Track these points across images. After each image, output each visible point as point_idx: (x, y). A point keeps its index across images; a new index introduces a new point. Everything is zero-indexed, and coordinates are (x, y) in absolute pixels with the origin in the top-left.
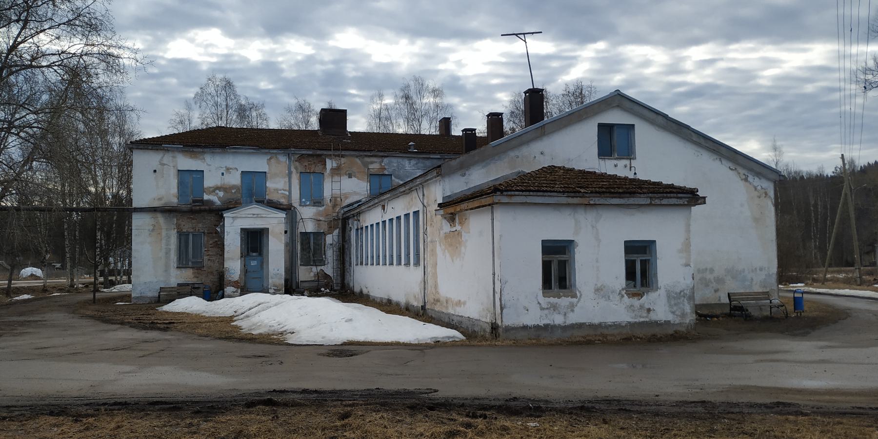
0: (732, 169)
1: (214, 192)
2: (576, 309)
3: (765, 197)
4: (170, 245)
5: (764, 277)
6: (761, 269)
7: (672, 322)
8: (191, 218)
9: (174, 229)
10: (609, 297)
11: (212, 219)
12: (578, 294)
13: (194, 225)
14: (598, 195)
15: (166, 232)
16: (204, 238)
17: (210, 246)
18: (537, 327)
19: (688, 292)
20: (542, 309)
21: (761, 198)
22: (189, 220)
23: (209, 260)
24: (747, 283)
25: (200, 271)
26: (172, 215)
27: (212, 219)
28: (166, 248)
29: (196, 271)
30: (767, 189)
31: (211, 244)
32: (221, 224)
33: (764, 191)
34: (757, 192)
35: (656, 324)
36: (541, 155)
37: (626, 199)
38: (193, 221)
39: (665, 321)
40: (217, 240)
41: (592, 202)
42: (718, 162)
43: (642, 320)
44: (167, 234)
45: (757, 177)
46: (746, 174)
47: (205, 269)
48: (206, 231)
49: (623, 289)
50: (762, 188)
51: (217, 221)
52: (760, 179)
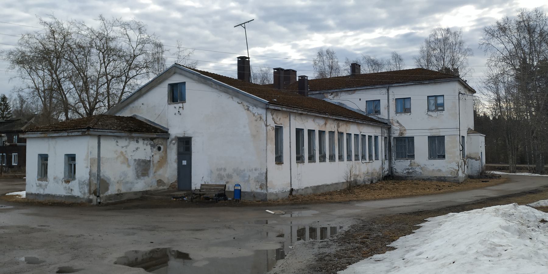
0: (239, 103)
2: (47, 187)
3: (260, 120)
5: (257, 175)
6: (256, 170)
7: (80, 197)
10: (58, 182)
12: (48, 181)
14: (54, 132)
18: (35, 194)
19: (87, 182)
20: (37, 186)
21: (257, 121)
24: (247, 179)
30: (261, 114)
33: (259, 116)
34: (255, 117)
35: (73, 197)
36: (143, 105)
37: (59, 134)
39: (77, 196)
41: (48, 136)
42: (231, 99)
43: (69, 194)
45: (255, 107)
46: (248, 105)
49: (63, 179)
50: (258, 114)
52: (257, 108)
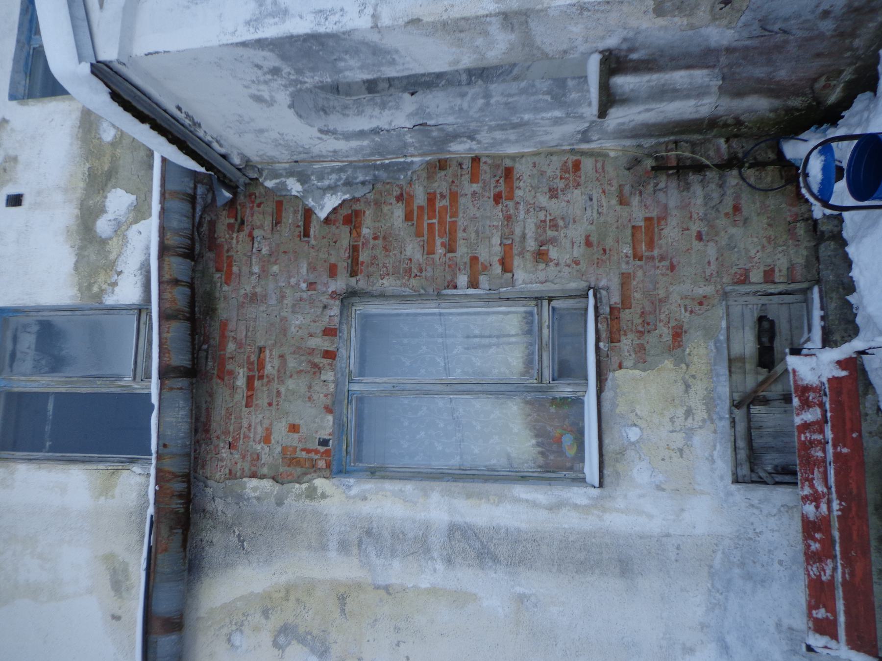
1: (104, 242)
4: (427, 526)
8: (250, 380)
9: (311, 494)
11: (265, 251)
13: (292, 363)
15: (333, 554)
16: (383, 296)
17: (440, 251)
22: (262, 399)
23: (541, 256)
25: (625, 315)
26: (219, 505)
27: (265, 251)
28: (449, 561)
29: (627, 343)
31: (431, 252)
32: (294, 187)
38: (268, 369)
40: (398, 212)
44: (344, 547)
47: (609, 280)
48: (339, 284)
51: (277, 222)
